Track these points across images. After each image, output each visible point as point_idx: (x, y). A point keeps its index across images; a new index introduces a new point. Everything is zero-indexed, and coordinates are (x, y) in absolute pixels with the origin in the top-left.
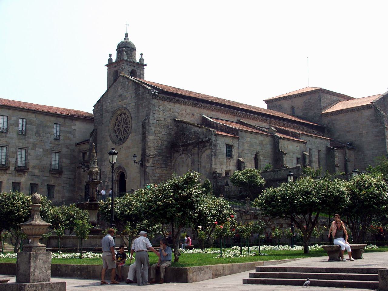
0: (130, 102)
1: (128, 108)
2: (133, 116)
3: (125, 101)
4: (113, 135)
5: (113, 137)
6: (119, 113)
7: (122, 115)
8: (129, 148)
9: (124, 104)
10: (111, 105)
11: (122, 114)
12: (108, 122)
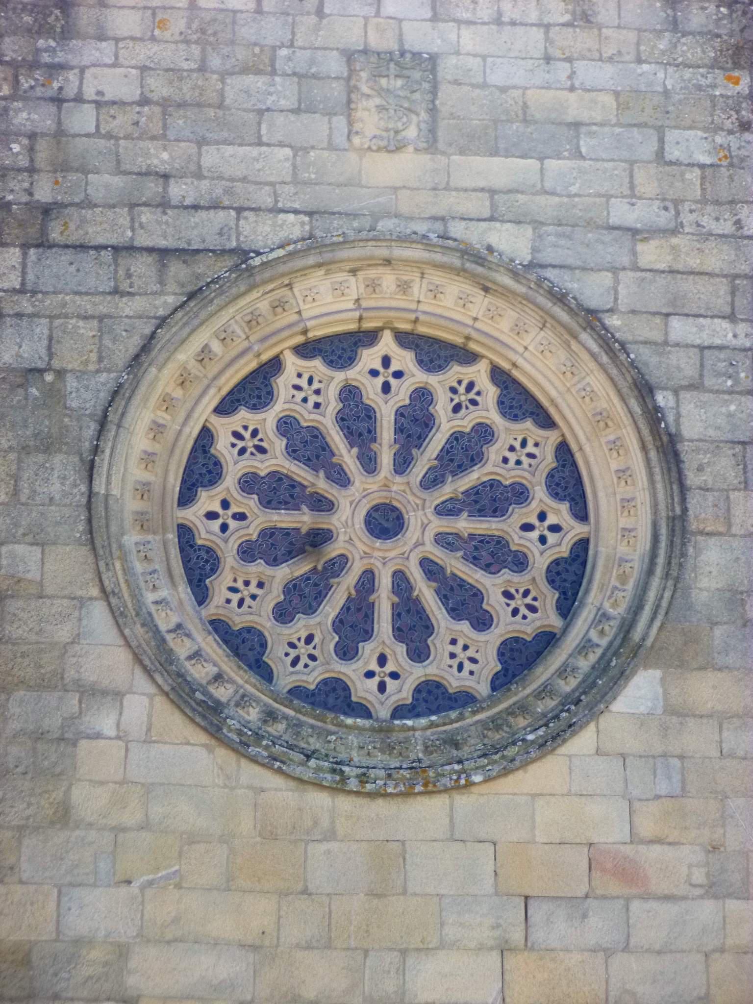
0: (622, 213)
1: (592, 289)
2: (694, 419)
3: (500, 170)
4: (168, 599)
5: (182, 649)
6: (326, 301)
7: (370, 358)
8: (614, 873)
9: (479, 205)
10: (161, 158)
11: (370, 337)
12: (84, 396)
